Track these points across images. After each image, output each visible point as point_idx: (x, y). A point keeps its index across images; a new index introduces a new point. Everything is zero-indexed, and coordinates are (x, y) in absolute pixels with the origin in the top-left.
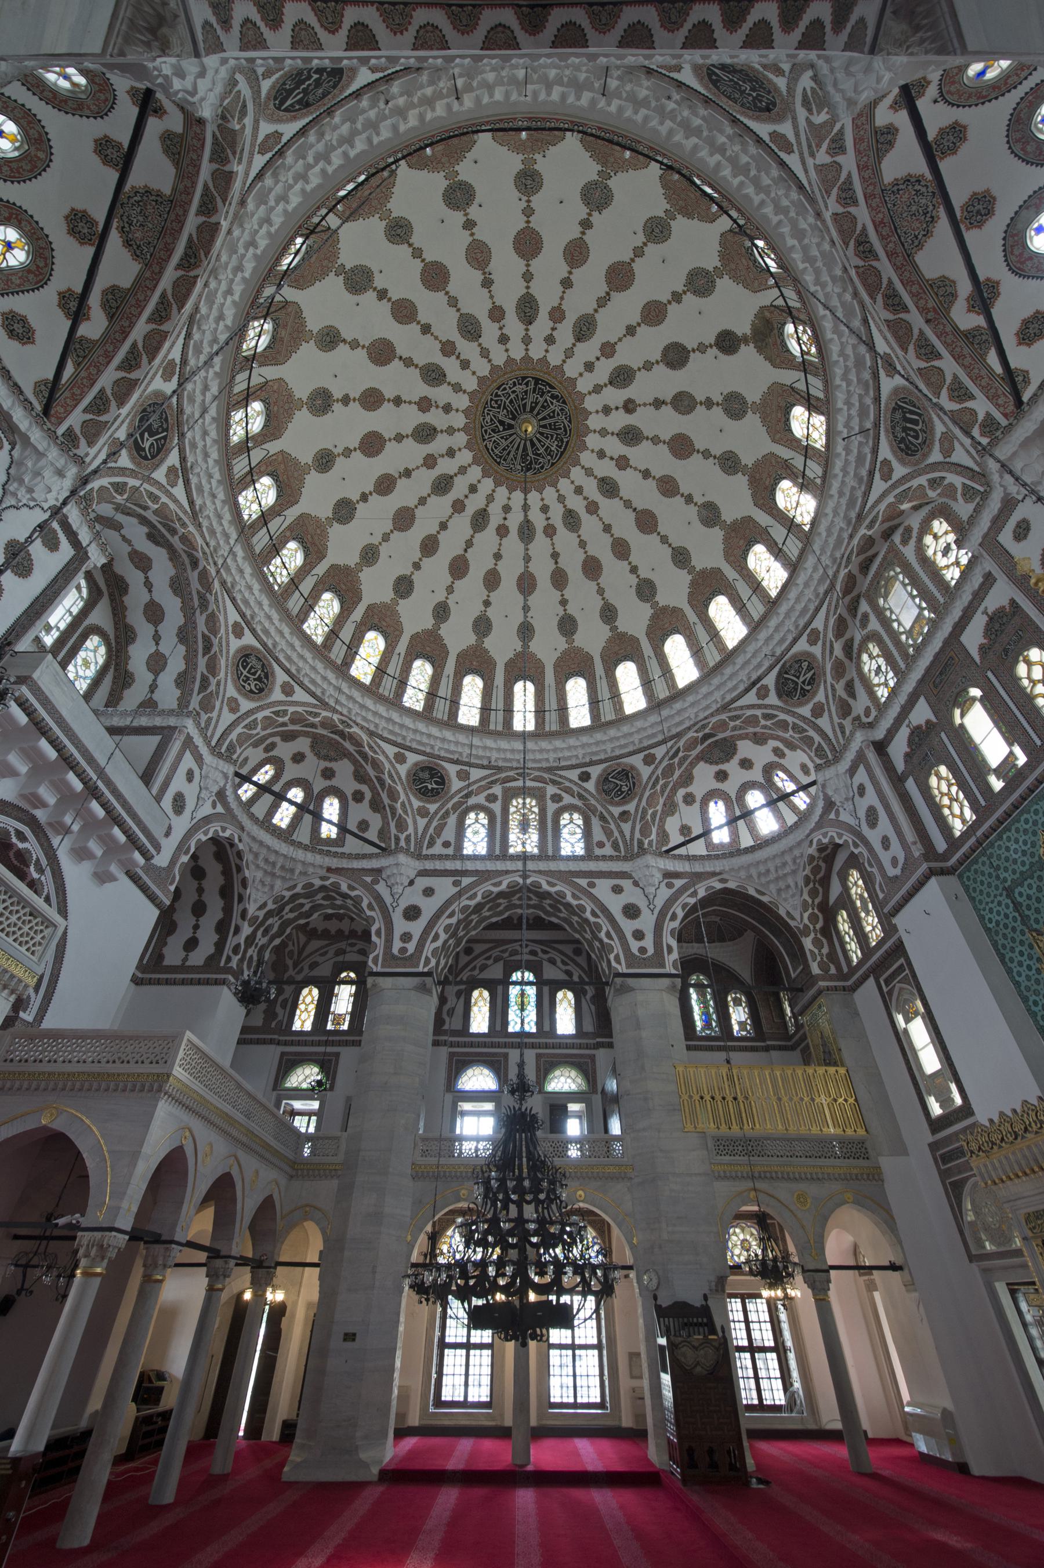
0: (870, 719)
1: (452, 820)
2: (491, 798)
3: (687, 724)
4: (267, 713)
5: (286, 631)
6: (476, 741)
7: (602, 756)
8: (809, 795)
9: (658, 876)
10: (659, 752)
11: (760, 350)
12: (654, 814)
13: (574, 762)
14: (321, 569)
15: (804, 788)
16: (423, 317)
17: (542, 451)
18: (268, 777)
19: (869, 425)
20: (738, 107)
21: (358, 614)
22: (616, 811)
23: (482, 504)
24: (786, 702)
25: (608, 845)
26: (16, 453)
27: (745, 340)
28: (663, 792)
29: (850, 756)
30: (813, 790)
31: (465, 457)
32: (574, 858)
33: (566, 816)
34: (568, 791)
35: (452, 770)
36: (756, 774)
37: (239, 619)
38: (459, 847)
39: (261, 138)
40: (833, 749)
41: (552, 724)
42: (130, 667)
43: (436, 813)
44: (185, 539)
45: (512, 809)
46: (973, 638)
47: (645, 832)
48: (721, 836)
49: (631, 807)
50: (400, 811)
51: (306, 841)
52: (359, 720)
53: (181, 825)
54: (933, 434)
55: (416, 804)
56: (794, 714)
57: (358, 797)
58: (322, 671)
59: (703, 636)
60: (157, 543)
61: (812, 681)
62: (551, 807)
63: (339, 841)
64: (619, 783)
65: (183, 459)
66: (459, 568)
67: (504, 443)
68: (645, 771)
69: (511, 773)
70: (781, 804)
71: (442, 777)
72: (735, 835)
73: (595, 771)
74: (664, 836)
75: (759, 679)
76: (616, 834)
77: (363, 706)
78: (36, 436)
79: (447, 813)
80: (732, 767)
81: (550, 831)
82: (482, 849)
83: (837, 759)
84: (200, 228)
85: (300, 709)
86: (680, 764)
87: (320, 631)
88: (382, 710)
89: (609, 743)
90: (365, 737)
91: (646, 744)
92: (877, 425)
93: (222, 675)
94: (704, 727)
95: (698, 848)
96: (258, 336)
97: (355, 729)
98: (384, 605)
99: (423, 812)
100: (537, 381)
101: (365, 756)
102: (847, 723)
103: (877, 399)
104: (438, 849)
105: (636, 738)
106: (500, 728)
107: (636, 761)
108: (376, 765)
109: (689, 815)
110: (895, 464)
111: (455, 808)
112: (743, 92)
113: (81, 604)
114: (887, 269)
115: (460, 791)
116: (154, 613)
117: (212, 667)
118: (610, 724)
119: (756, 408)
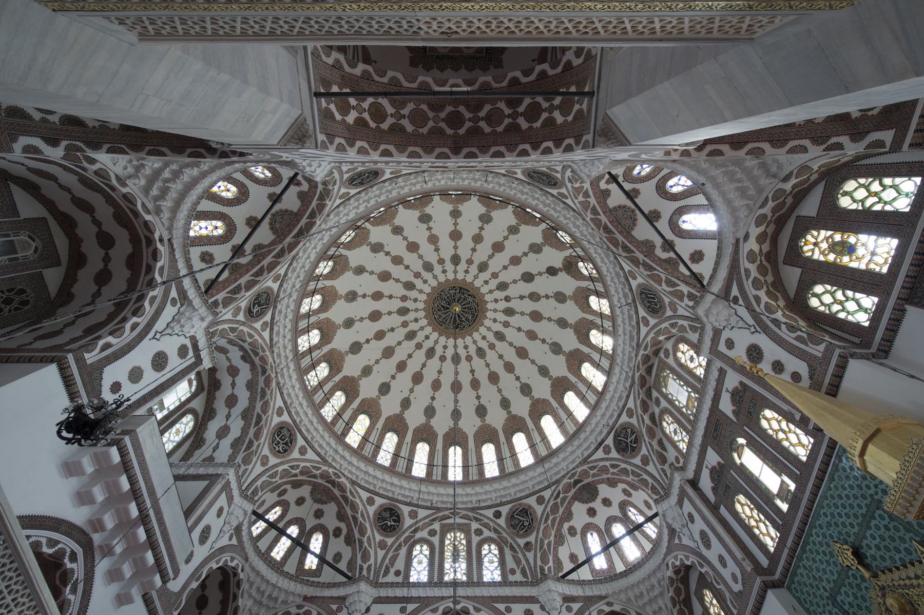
0: (681, 465)
1: (403, 551)
2: (432, 533)
3: (562, 473)
4: (286, 467)
5: (310, 412)
6: (423, 488)
7: (509, 499)
8: (655, 525)
9: (559, 600)
10: (547, 494)
12: (549, 544)
13: (489, 503)
14: (337, 378)
15: (649, 519)
16: (406, 263)
18: (276, 517)
19: (630, 301)
21: (355, 404)
22: (522, 542)
23: (432, 345)
24: (623, 456)
25: (518, 572)
26: (182, 309)
27: (560, 270)
28: (553, 525)
29: (675, 491)
30: (657, 520)
31: (424, 322)
32: (493, 584)
33: (486, 547)
34: (486, 526)
35: (406, 510)
36: (615, 511)
37: (282, 405)
38: (407, 575)
39: (341, 193)
40: (663, 488)
41: (474, 476)
42: (205, 436)
43: (392, 546)
44: (263, 359)
45: (447, 542)
46: (726, 406)
47: (545, 560)
48: (600, 563)
49: (531, 538)
50: (366, 544)
51: (293, 572)
52: (346, 473)
53: (201, 553)
55: (378, 537)
56: (630, 464)
57: (337, 532)
58: (327, 439)
59: (564, 416)
60: (245, 361)
61: (636, 441)
62: (475, 539)
63: (317, 572)
64: (521, 520)
65: (273, 318)
66: (417, 378)
67: (444, 316)
68: (539, 509)
69: (447, 513)
70: (636, 533)
71: (398, 516)
72: (610, 560)
73: (505, 510)
74: (558, 564)
75: (603, 441)
76: (523, 562)
77: (350, 463)
78: (197, 302)
79: (400, 545)
80: (597, 504)
81: (475, 561)
82: (424, 578)
83: (667, 495)
84: (306, 224)
85: (308, 464)
86: (562, 503)
87: (330, 414)
88: (362, 465)
89: (512, 489)
90: (348, 485)
91: (537, 488)
92: (634, 301)
93: (263, 440)
94: (573, 475)
95: (584, 573)
96: (325, 268)
97: (343, 480)
98: (372, 399)
99: (382, 545)
100: (461, 288)
101: (346, 499)
102: (666, 467)
103: (631, 290)
104: (391, 578)
105: (530, 484)
106: (439, 478)
107: (532, 501)
108: (354, 507)
109: (572, 545)
110: (649, 318)
111: (406, 542)
113: (189, 395)
115: (410, 527)
116: (231, 401)
117: (257, 435)
118: (511, 474)
119: (571, 298)
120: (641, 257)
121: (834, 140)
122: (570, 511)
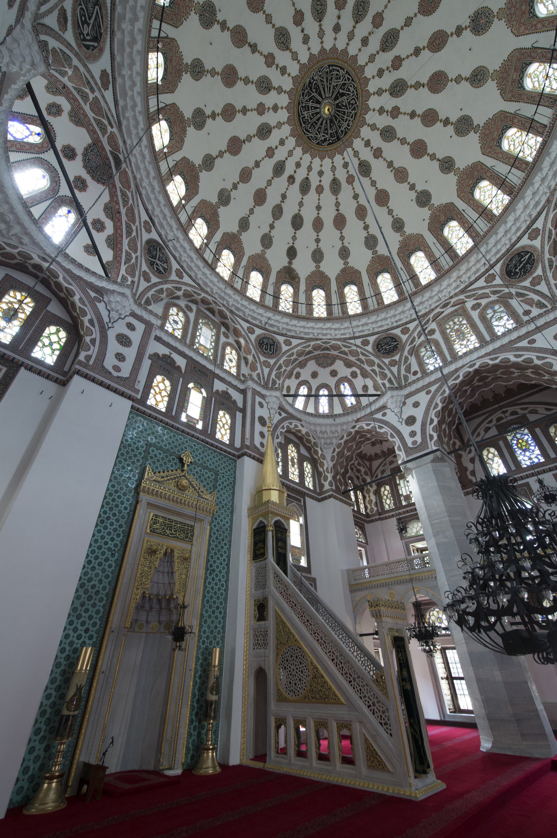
11: (285, 268)
17: (310, 104)
19: (267, 326)
20: (381, 338)
27: (290, 263)
28: (79, 91)
46: (218, 386)
54: (269, 358)
100: (338, 139)
112: (386, 344)
114: (316, 353)
120: (301, 359)
122: (82, 125)
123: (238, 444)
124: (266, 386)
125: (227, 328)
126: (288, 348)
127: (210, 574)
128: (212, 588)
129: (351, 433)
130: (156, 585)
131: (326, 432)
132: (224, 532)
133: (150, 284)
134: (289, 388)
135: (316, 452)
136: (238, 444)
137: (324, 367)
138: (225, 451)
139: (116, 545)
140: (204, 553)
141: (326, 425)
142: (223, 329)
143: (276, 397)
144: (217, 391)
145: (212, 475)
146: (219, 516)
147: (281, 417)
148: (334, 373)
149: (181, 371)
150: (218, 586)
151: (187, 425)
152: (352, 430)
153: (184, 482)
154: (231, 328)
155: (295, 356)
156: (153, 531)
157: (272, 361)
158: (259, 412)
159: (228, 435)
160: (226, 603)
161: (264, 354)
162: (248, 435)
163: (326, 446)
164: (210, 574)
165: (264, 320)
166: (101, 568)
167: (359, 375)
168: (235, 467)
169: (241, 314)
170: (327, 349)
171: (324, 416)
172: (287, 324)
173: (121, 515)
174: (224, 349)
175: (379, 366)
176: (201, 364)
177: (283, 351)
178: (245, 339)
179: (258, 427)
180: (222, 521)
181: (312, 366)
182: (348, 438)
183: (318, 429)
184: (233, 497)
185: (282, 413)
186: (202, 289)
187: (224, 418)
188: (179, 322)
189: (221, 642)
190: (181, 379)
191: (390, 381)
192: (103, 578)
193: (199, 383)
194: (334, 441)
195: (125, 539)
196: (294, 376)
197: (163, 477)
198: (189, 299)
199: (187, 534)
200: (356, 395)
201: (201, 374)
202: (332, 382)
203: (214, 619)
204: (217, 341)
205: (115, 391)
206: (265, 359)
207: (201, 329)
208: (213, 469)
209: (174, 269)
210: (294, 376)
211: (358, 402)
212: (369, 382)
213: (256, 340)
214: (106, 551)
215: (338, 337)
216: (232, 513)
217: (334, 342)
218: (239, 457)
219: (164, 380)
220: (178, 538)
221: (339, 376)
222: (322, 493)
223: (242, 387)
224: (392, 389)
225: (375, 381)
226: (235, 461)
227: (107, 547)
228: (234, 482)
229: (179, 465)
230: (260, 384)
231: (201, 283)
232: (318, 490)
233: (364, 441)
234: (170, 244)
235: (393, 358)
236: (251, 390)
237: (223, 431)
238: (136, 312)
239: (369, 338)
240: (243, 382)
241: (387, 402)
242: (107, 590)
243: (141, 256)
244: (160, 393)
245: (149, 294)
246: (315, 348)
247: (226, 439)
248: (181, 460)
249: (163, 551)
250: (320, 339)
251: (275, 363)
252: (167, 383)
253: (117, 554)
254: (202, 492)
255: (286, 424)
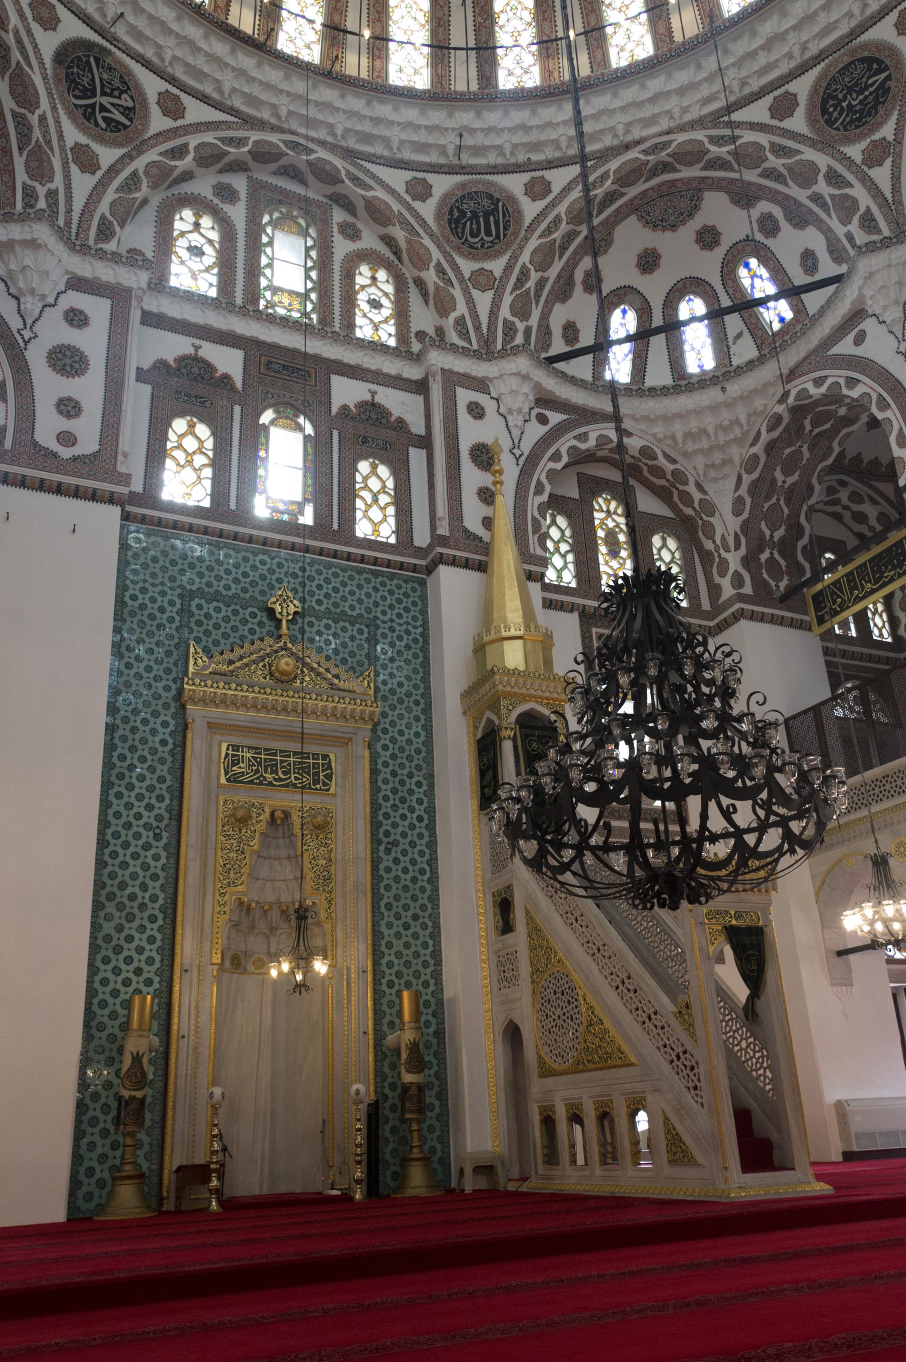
19: (467, 159)
20: (834, 71)
46: (346, 393)
54: (488, 257)
61: (114, 126)
103: (494, 170)
112: (850, 90)
114: (633, 192)
121: (743, 540)
123: (422, 538)
124: (487, 353)
125: (348, 206)
126: (540, 205)
127: (388, 851)
128: (397, 879)
129: (778, 418)
130: (269, 884)
131: (704, 431)
132: (410, 759)
133: (99, 174)
134: (570, 331)
135: (686, 498)
136: (422, 538)
137: (673, 227)
138: (389, 564)
139: (159, 818)
140: (363, 808)
141: (697, 412)
142: (339, 216)
143: (518, 374)
144: (345, 408)
145: (360, 632)
146: (393, 724)
147: (546, 429)
148: (708, 238)
149: (233, 388)
150: (411, 874)
151: (276, 525)
152: (780, 409)
153: (286, 663)
154: (360, 205)
155: (564, 227)
156: (233, 779)
157: (497, 266)
158: (471, 433)
159: (392, 521)
160: (436, 906)
161: (472, 252)
162: (442, 510)
163: (713, 474)
164: (388, 851)
165: (450, 141)
166: (139, 862)
167: (784, 224)
168: (424, 598)
169: (378, 149)
170: (666, 167)
171: (705, 381)
172: (524, 128)
173: (156, 757)
174: (349, 276)
175: (834, 178)
176: (286, 349)
177: (528, 219)
178: (405, 225)
179: (472, 477)
180: (401, 733)
181: (632, 236)
182: (775, 434)
183: (679, 429)
184: (427, 673)
185: (548, 413)
186: (249, 122)
187: (374, 479)
188: (207, 249)
189: (432, 982)
190: (237, 409)
191: (868, 223)
192: (148, 881)
193: (288, 404)
194: (737, 453)
195: (176, 803)
196: (579, 288)
197: (231, 662)
198: (219, 166)
199: (314, 773)
200: (790, 292)
201: (287, 376)
202: (708, 266)
203: (410, 939)
204: (324, 265)
205: (76, 493)
206: (476, 266)
207: (270, 244)
208: (360, 615)
209: (152, 98)
210: (579, 288)
211: (799, 310)
212: (814, 239)
213: (438, 216)
214: (141, 830)
215: (695, 113)
216: (427, 710)
217: (681, 137)
218: (430, 570)
219: (192, 426)
220: (295, 786)
221: (727, 242)
222: (717, 609)
223: (413, 372)
224: (871, 248)
225: (827, 232)
226: (422, 583)
227: (141, 823)
228: (425, 636)
229: (269, 625)
230: (465, 352)
231: (238, 103)
232: (706, 605)
233: (834, 431)
234: (120, 31)
235: (877, 136)
236: (439, 378)
237: (375, 514)
238: (80, 273)
239: (792, 87)
240: (417, 358)
241: (861, 296)
242: (161, 901)
243: (54, 109)
244: (190, 462)
245: (104, 208)
246: (626, 178)
247: (387, 533)
248: (271, 612)
249: (265, 817)
250: (638, 143)
251: (508, 269)
252: (203, 430)
253: (165, 835)
254: (337, 676)
255: (565, 444)
